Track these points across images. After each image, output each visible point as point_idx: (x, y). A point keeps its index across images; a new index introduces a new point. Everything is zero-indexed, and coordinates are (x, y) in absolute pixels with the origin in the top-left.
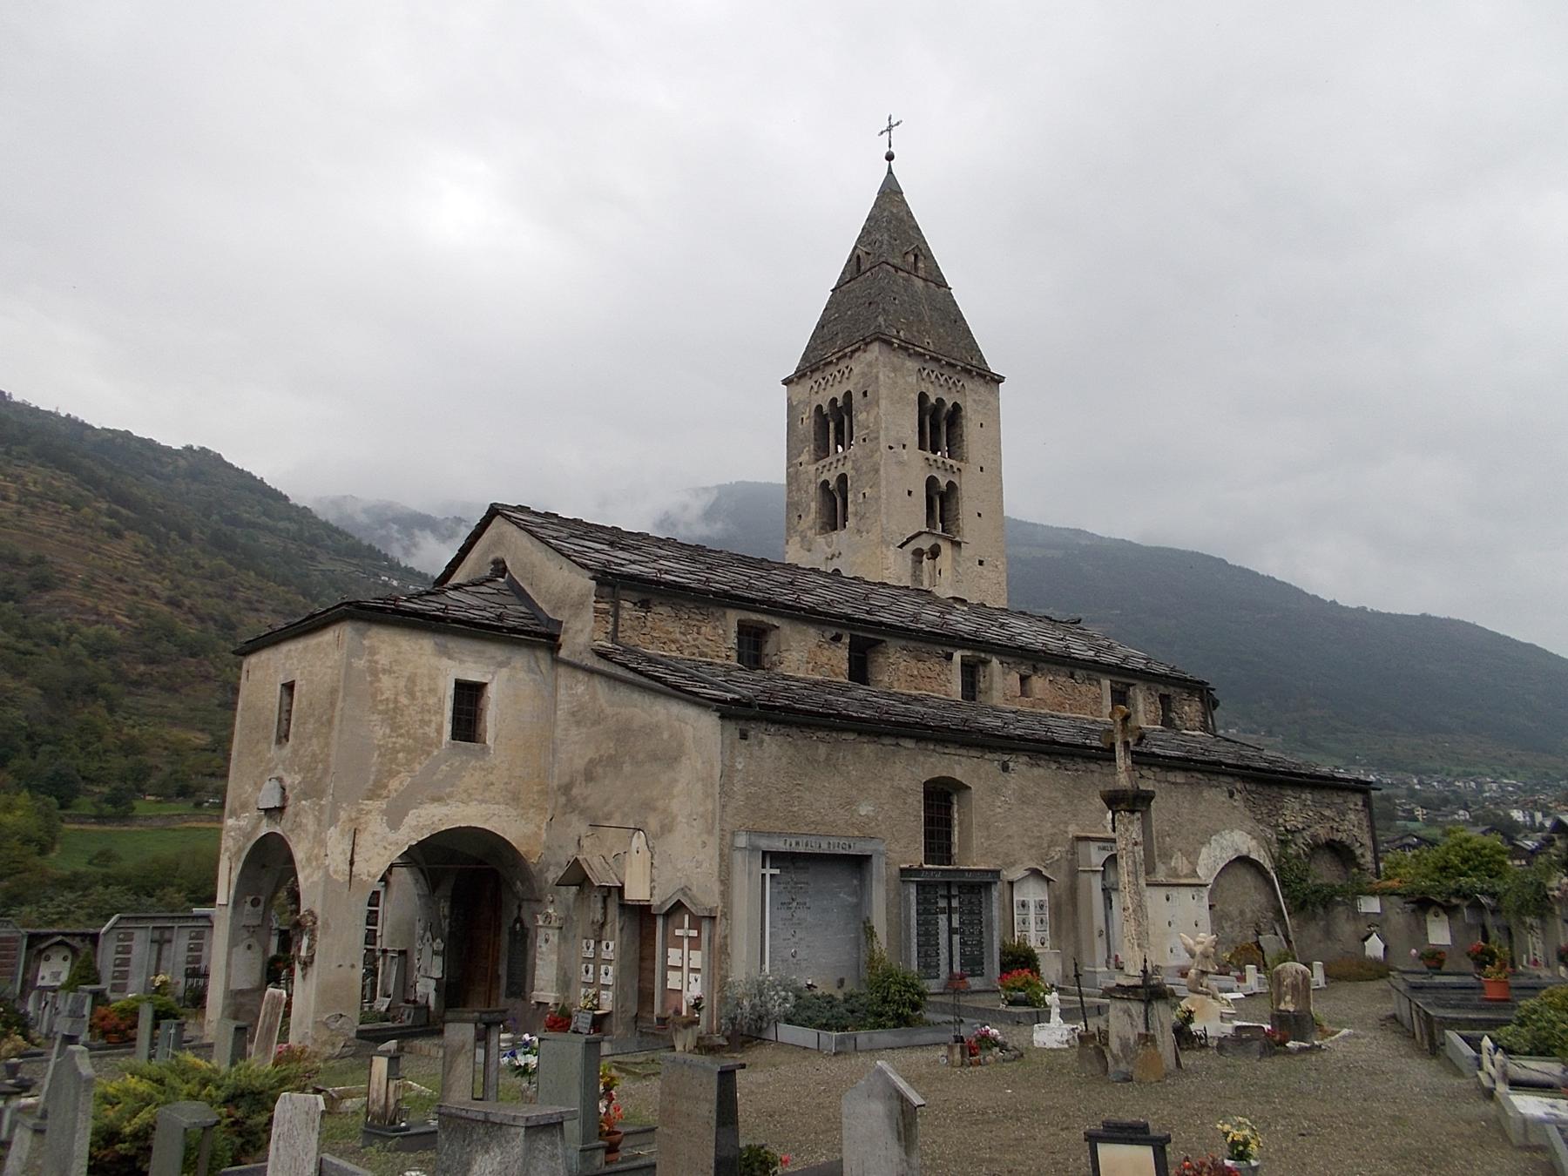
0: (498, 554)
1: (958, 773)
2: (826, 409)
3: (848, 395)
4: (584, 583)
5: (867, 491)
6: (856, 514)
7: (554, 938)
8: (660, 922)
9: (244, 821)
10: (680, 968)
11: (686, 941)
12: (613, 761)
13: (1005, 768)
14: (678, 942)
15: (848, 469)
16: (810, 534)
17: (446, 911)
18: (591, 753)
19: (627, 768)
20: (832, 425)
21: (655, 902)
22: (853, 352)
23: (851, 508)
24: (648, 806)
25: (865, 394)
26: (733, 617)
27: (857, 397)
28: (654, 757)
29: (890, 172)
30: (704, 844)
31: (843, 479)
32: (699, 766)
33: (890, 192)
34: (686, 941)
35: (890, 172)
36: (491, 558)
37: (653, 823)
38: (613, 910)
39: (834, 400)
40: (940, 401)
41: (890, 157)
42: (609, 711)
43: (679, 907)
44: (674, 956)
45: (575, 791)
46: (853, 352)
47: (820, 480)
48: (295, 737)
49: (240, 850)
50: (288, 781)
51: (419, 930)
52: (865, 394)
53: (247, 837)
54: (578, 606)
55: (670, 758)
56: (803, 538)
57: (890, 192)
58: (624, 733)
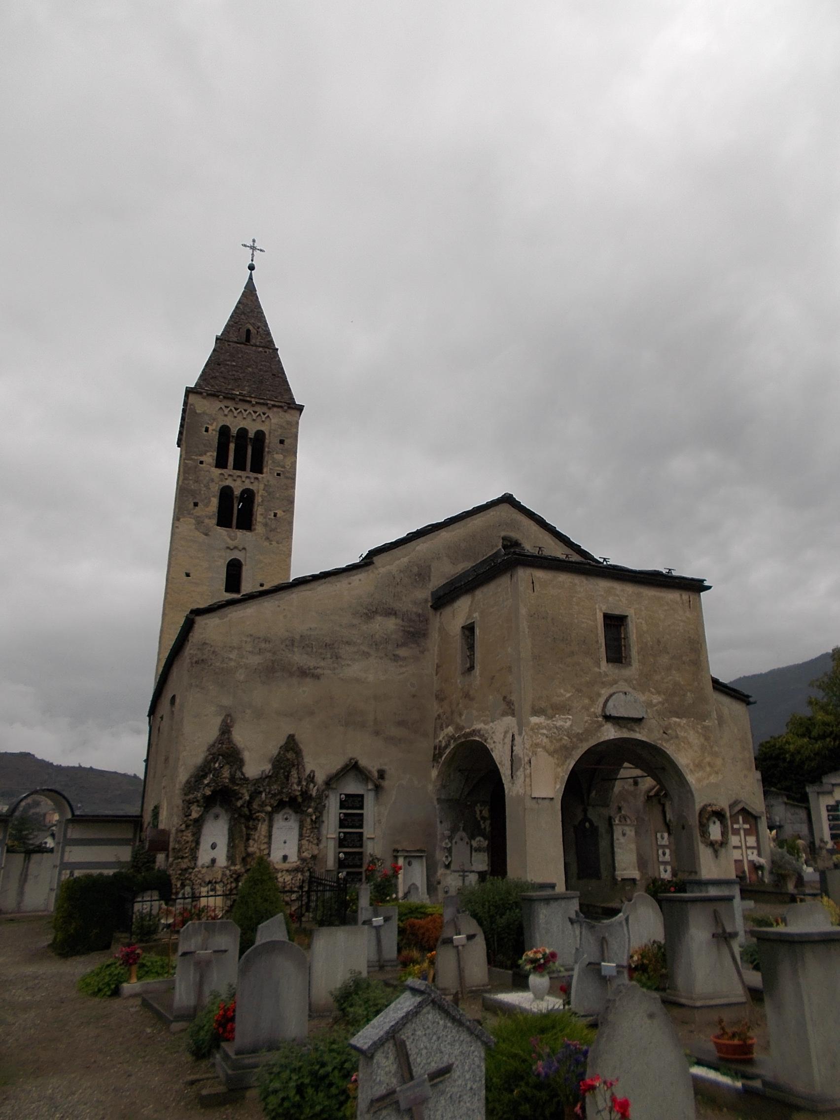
0: (514, 535)
5: (280, 513)
7: (631, 832)
10: (747, 848)
11: (742, 832)
14: (736, 832)
17: (486, 813)
20: (232, 446)
22: (274, 406)
25: (282, 442)
29: (251, 278)
30: (746, 776)
32: (736, 731)
33: (250, 290)
34: (742, 832)
35: (251, 278)
36: (503, 534)
39: (243, 432)
41: (251, 268)
46: (274, 406)
51: (442, 829)
52: (282, 442)
53: (580, 738)
56: (199, 522)
57: (250, 290)
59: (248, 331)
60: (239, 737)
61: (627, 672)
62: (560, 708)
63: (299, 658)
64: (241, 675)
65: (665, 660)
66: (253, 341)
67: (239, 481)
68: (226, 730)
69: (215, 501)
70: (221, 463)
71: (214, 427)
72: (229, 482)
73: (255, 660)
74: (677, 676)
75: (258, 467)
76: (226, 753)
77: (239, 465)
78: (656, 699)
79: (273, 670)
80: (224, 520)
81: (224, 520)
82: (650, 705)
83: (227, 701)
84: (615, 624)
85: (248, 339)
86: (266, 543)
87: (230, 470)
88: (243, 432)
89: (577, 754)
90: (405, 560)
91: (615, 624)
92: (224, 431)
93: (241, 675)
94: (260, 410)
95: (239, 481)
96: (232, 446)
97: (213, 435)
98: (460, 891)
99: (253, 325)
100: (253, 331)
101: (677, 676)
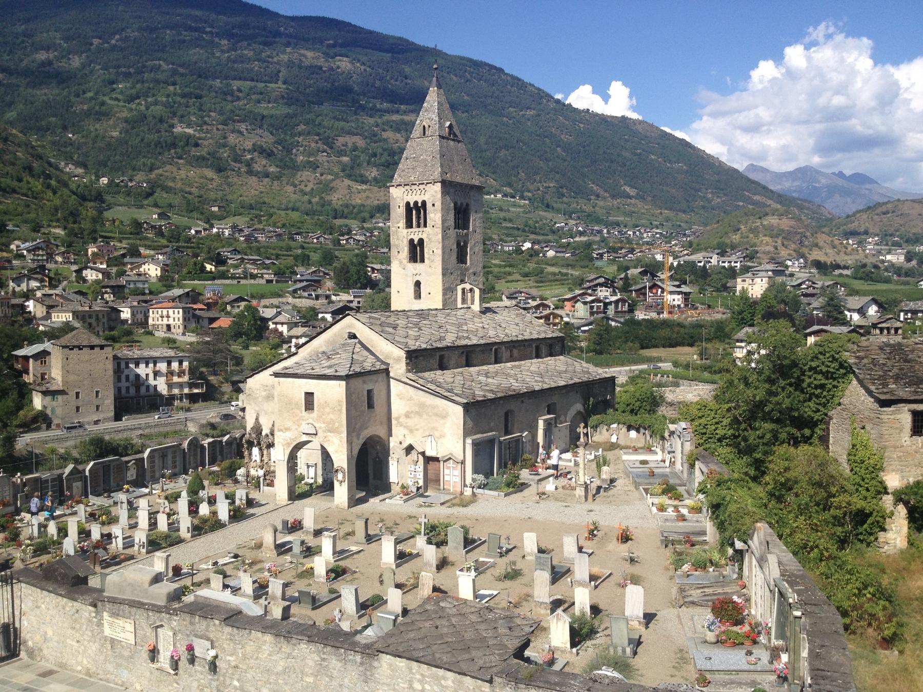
0: (353, 331)
1: (512, 408)
2: (412, 205)
3: (424, 203)
4: (403, 355)
6: (429, 259)
8: (442, 463)
9: (288, 435)
12: (418, 414)
13: (522, 402)
14: (449, 468)
15: (424, 237)
16: (405, 261)
18: (407, 409)
19: (425, 416)
20: (414, 212)
23: (426, 255)
24: (434, 429)
26: (438, 354)
27: (429, 206)
28: (436, 415)
31: (421, 241)
37: (437, 434)
38: (421, 458)
39: (416, 203)
40: (462, 204)
42: (415, 397)
43: (450, 459)
44: (447, 471)
45: (401, 420)
47: (410, 237)
48: (318, 411)
49: (289, 444)
50: (317, 425)
54: (398, 360)
55: (444, 417)
56: (401, 263)
58: (422, 405)
60: (261, 421)
62: (287, 429)
64: (260, 399)
65: (327, 410)
67: (416, 234)
68: (257, 419)
70: (409, 225)
71: (403, 205)
72: (412, 236)
73: (264, 394)
74: (332, 416)
75: (425, 226)
82: (320, 428)
84: (309, 396)
86: (430, 270)
87: (415, 229)
88: (416, 203)
89: (292, 446)
90: (309, 350)
91: (309, 396)
93: (260, 399)
94: (421, 187)
95: (416, 234)
96: (414, 212)
97: (402, 211)
98: (705, 444)
101: (332, 416)
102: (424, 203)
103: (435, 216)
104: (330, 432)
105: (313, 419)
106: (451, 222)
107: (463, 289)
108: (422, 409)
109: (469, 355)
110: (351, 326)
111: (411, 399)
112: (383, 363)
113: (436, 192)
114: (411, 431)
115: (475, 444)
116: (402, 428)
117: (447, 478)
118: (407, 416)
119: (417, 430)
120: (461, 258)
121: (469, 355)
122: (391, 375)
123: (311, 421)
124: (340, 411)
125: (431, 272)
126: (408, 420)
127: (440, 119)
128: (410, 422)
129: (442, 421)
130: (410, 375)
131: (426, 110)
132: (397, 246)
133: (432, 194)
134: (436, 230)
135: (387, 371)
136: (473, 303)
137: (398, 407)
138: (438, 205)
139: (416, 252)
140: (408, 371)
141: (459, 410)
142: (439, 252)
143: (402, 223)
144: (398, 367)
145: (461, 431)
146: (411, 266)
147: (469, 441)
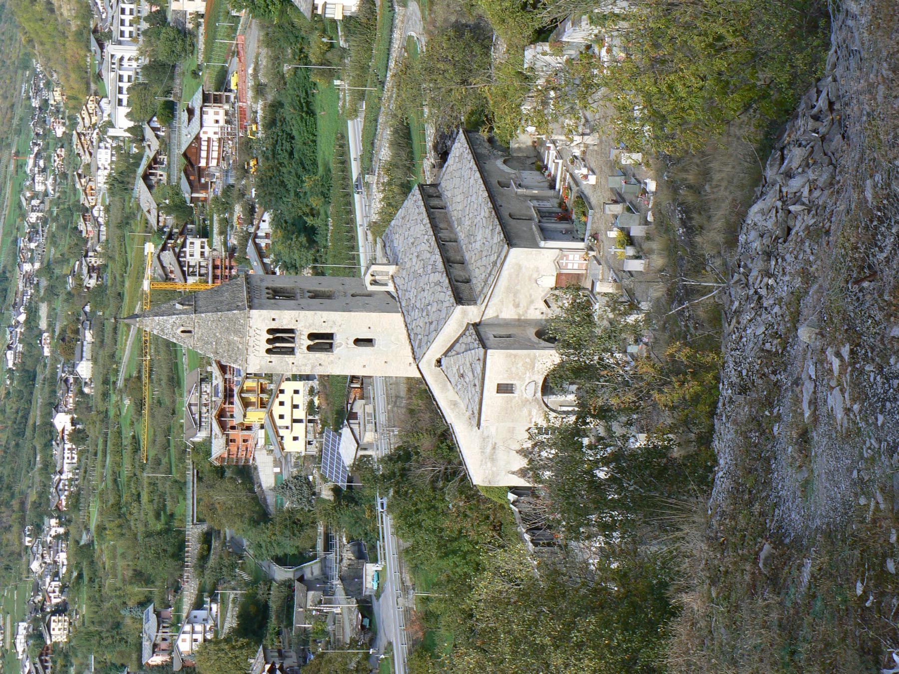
0: (434, 362)
4: (460, 308)
12: (516, 294)
14: (567, 264)
15: (306, 333)
18: (511, 306)
19: (518, 287)
21: (555, 274)
25: (274, 320)
27: (274, 325)
28: (518, 275)
31: (312, 336)
37: (535, 276)
39: (269, 341)
47: (306, 351)
52: (274, 320)
54: (465, 313)
55: (519, 267)
58: (509, 290)
59: (183, 332)
60: (516, 468)
61: (518, 386)
63: (489, 450)
64: (494, 469)
65: (514, 369)
66: (190, 329)
68: (513, 473)
69: (318, 355)
70: (291, 351)
72: (305, 348)
73: (489, 464)
74: (520, 365)
76: (523, 473)
77: (292, 340)
78: (528, 375)
79: (493, 459)
80: (329, 348)
81: (329, 348)
82: (530, 377)
83: (503, 473)
85: (190, 332)
88: (269, 341)
92: (269, 351)
93: (494, 469)
97: (275, 358)
99: (178, 328)
100: (182, 329)
101: (520, 365)
102: (270, 331)
103: (285, 318)
104: (534, 368)
105: (521, 386)
106: (292, 303)
107: (375, 282)
108: (513, 291)
109: (452, 260)
110: (429, 363)
111: (502, 302)
112: (467, 329)
113: (260, 316)
114: (532, 302)
115: (545, 239)
116: (529, 312)
117: (576, 267)
118: (517, 306)
119: (531, 296)
120: (327, 296)
121: (452, 260)
122: (478, 321)
123: (524, 387)
124: (515, 356)
125: (344, 324)
126: (521, 305)
127: (174, 314)
128: (523, 303)
129: (524, 270)
130: (479, 302)
131: (162, 330)
132: (313, 367)
133: (261, 321)
134: (301, 318)
135: (476, 326)
136: (387, 273)
137: (509, 313)
138: (274, 313)
139: (322, 342)
140: (475, 304)
141: (514, 251)
142: (326, 315)
143: (288, 359)
144: (471, 314)
145: (534, 251)
146: (336, 351)
147: (542, 244)
